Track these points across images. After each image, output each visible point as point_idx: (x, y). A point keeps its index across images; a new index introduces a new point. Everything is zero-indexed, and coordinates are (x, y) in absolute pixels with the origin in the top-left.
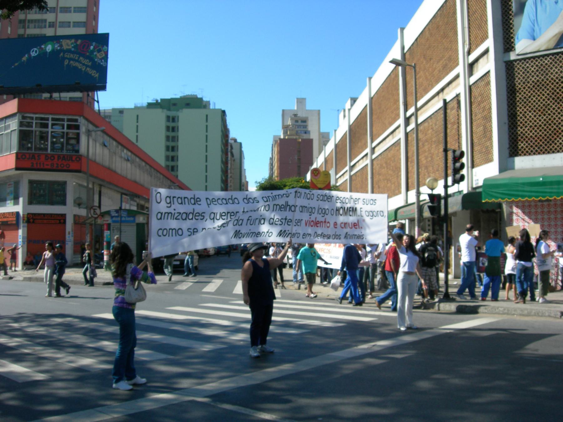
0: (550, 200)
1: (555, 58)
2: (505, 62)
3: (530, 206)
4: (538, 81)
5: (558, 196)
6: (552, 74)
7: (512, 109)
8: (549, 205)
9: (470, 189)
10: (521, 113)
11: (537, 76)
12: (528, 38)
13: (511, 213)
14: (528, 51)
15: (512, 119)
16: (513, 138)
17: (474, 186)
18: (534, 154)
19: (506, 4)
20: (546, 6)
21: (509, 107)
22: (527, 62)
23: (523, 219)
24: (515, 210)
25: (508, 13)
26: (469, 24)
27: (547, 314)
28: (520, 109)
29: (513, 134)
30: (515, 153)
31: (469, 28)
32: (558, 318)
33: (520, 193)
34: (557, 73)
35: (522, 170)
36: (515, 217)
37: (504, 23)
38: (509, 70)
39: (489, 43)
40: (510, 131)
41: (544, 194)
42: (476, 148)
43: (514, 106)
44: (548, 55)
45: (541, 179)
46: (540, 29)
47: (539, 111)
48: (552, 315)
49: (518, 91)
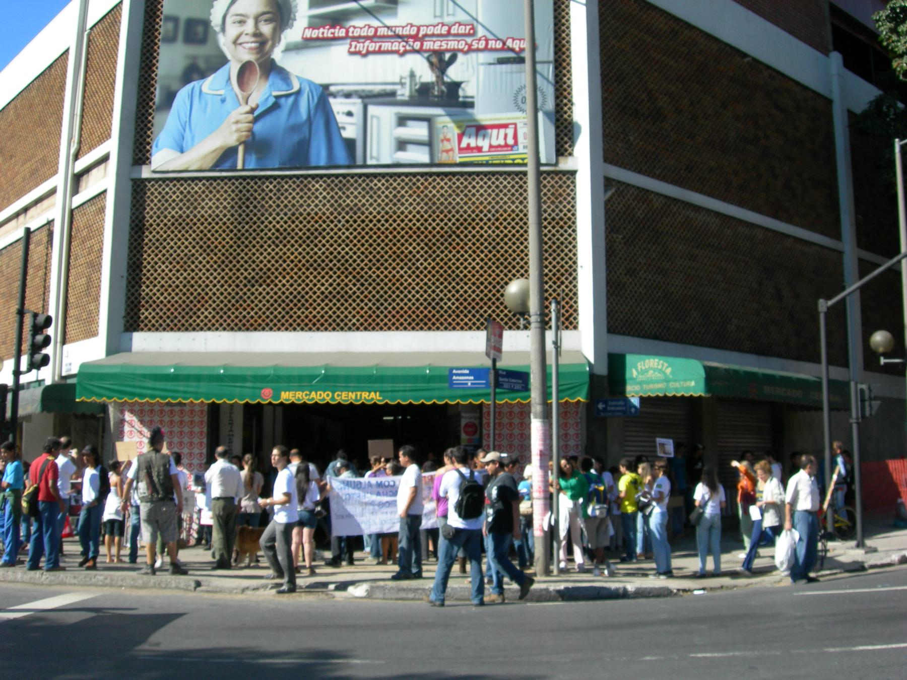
0: (185, 404)
2: (133, 180)
3: (152, 411)
4: (181, 216)
5: (197, 399)
6: (203, 208)
7: (135, 255)
8: (182, 411)
9: (56, 378)
10: (149, 263)
11: (181, 209)
12: (173, 148)
13: (122, 422)
14: (170, 169)
15: (134, 271)
16: (132, 302)
17: (64, 374)
18: (164, 329)
19: (146, 90)
20: (206, 105)
21: (131, 251)
22: (168, 185)
23: (140, 432)
24: (128, 416)
25: (148, 104)
26: (83, 110)
27: (174, 585)
28: (148, 258)
29: (133, 294)
30: (135, 326)
31: (82, 116)
32: (190, 590)
33: (137, 391)
34: (210, 208)
35: (142, 354)
36: (127, 428)
37: (139, 118)
38: (138, 193)
39: (111, 146)
40: (129, 291)
41: (174, 395)
42: (71, 312)
43: (139, 252)
44: (200, 179)
45: (172, 370)
46: (193, 138)
48: (182, 586)
49: (148, 229)
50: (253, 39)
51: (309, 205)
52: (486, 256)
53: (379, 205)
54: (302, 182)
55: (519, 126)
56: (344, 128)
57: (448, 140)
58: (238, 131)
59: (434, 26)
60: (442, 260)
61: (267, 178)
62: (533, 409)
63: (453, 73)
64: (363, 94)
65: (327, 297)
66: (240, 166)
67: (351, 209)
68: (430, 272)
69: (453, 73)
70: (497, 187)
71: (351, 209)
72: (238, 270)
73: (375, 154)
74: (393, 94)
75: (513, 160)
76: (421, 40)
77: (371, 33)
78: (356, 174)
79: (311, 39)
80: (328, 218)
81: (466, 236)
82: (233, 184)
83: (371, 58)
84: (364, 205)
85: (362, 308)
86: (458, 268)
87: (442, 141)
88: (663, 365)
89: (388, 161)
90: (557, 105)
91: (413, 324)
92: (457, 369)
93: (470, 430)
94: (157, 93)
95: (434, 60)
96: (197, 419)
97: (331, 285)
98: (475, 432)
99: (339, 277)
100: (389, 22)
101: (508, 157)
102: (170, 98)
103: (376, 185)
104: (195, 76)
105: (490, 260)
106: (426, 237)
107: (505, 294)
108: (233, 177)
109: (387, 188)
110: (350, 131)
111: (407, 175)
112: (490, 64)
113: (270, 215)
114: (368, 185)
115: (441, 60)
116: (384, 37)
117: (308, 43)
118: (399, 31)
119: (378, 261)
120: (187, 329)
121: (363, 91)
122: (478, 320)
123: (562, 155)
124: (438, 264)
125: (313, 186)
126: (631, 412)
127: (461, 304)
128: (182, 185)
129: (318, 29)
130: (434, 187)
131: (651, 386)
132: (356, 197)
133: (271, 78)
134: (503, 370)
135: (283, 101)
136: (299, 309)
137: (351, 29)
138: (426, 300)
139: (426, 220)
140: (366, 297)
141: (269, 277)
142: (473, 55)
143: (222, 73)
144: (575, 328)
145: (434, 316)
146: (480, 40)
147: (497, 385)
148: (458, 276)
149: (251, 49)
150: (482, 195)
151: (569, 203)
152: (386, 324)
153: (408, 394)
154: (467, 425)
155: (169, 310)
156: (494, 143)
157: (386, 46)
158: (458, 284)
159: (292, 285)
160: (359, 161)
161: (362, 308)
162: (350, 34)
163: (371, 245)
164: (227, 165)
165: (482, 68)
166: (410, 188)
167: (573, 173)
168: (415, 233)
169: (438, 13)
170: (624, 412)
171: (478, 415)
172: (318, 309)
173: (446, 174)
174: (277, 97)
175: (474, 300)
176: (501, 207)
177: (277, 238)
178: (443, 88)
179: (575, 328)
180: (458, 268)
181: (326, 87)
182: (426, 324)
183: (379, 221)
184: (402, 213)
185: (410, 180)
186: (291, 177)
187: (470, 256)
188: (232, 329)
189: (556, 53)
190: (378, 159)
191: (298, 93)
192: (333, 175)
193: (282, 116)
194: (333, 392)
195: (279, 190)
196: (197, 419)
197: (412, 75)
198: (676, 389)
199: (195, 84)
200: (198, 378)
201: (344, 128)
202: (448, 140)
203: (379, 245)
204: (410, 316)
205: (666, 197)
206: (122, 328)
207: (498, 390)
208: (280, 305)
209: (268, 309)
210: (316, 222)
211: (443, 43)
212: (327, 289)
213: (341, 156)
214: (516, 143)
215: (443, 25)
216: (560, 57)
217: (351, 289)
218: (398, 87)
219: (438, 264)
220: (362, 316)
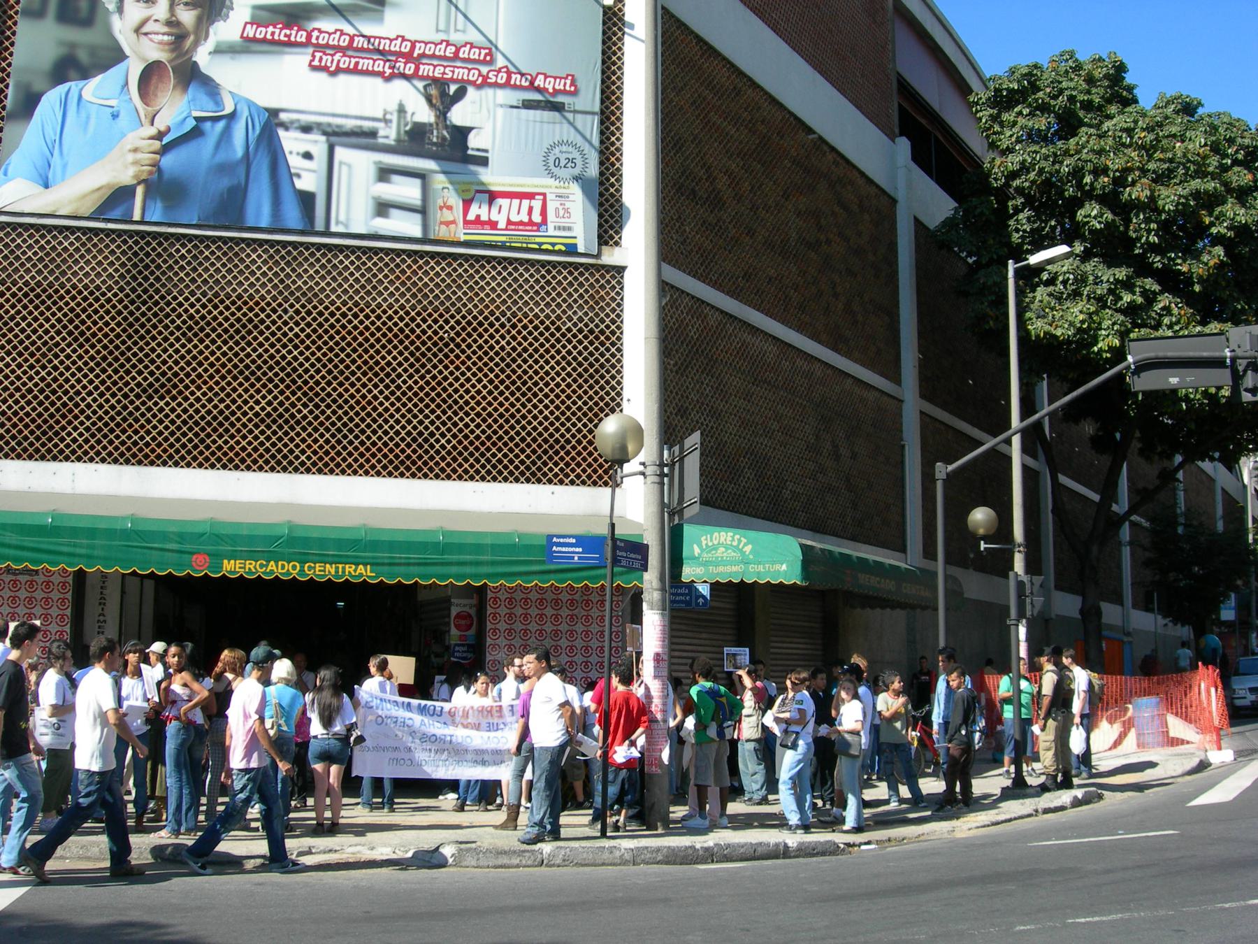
1: (90, 239)
4: (39, 284)
6: (75, 274)
20: (88, 118)
22: (19, 235)
34: (87, 275)
46: (65, 166)
50: (166, 29)
51: (240, 284)
52: (497, 376)
53: (345, 292)
54: (231, 248)
56: (299, 176)
57: (450, 208)
58: (135, 163)
59: (436, 45)
60: (434, 378)
62: (645, 596)
63: (459, 115)
64: (329, 130)
65: (263, 421)
66: (137, 217)
67: (304, 294)
68: (416, 394)
69: (459, 115)
70: (515, 280)
71: (304, 294)
72: (128, 372)
73: (342, 218)
74: (373, 134)
75: (540, 244)
76: (417, 61)
77: (344, 42)
78: (313, 244)
79: (254, 40)
80: (269, 304)
81: (469, 346)
82: (125, 242)
83: (342, 78)
84: (322, 290)
85: (316, 441)
86: (456, 391)
87: (441, 208)
88: (739, 540)
89: (363, 231)
90: (602, 174)
92: (558, 537)
93: (463, 622)
94: (10, 92)
95: (433, 91)
97: (269, 403)
98: (469, 627)
99: (282, 392)
100: (368, 29)
101: (532, 240)
102: (30, 102)
103: (341, 262)
104: (72, 73)
105: (502, 382)
106: (412, 343)
107: (596, 432)
108: (125, 232)
109: (358, 269)
110: (308, 181)
111: (387, 252)
112: (512, 107)
113: (181, 293)
114: (329, 261)
115: (443, 94)
116: (362, 50)
117: (249, 46)
118: (385, 45)
119: (342, 373)
120: (43, 458)
121: (329, 125)
122: (483, 466)
123: (606, 243)
124: (428, 383)
125: (248, 256)
126: (698, 604)
127: (460, 442)
128: (43, 236)
129: (267, 27)
130: (426, 273)
131: (721, 569)
132: (311, 277)
133: (191, 90)
134: (621, 540)
135: (207, 126)
137: (315, 34)
138: (409, 434)
139: (413, 319)
140: (321, 424)
141: (175, 386)
142: (489, 92)
143: (115, 73)
145: (420, 457)
146: (499, 71)
147: (616, 561)
148: (456, 402)
149: (161, 43)
150: (493, 290)
151: (613, 310)
152: (350, 466)
154: (458, 616)
155: (15, 426)
156: (514, 218)
157: (365, 64)
158: (456, 413)
159: (210, 400)
160: (320, 226)
161: (316, 441)
162: (314, 41)
163: (331, 349)
164: (116, 214)
165: (500, 111)
166: (392, 271)
167: (621, 270)
168: (396, 336)
169: (442, 27)
170: (688, 603)
171: (474, 601)
172: (250, 438)
173: (444, 256)
174: (196, 119)
175: (478, 438)
176: (520, 309)
177: (190, 328)
178: (445, 133)
180: (456, 391)
181: (274, 113)
182: (408, 469)
183: (344, 315)
184: (379, 306)
185: (392, 260)
186: (214, 240)
187: (474, 375)
188: (116, 461)
189: (602, 102)
190: (346, 226)
191: (232, 116)
192: (278, 242)
193: (204, 150)
194: (303, 563)
195: (195, 258)
196: (55, 595)
197: (401, 110)
199: (74, 86)
200: (91, 533)
201: (299, 176)
202: (450, 208)
203: (343, 350)
204: (385, 456)
205: (722, 312)
207: (616, 569)
208: (191, 429)
209: (172, 433)
210: (251, 309)
211: (447, 70)
212: (263, 409)
213: (292, 216)
214: (544, 221)
215: (448, 44)
216: (607, 108)
217: (299, 411)
218: (380, 125)
219: (428, 383)
220: (315, 453)
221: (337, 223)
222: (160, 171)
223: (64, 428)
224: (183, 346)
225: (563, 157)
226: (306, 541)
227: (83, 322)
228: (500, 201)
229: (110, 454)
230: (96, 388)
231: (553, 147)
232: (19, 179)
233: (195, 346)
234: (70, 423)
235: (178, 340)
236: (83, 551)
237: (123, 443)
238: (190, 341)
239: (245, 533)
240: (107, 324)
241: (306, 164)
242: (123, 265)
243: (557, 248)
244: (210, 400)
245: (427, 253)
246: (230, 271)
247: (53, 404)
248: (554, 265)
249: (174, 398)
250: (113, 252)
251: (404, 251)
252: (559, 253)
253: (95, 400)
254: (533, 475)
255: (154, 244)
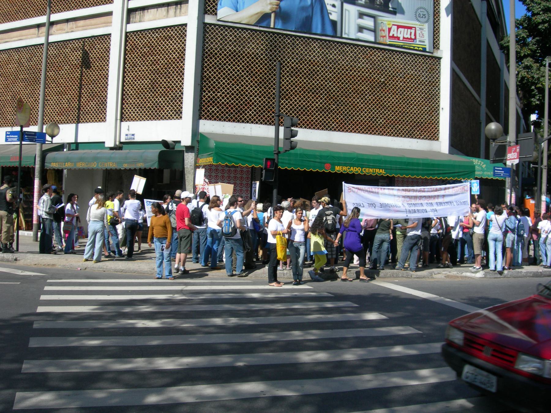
3: (217, 170)
4: (235, 51)
8: (236, 171)
9: (117, 143)
14: (230, 21)
17: (123, 140)
22: (227, 30)
33: (254, 160)
34: (253, 48)
44: (247, 30)
47: (233, 80)
48: (405, 276)
55: (417, 29)
61: (287, 35)
66: (272, 26)
72: (270, 89)
73: (347, 32)
75: (414, 47)
82: (267, 36)
87: (381, 30)
88: (481, 163)
89: (354, 38)
91: (323, 126)
96: (244, 176)
103: (346, 49)
108: (267, 32)
111: (362, 46)
113: (289, 58)
136: (304, 115)
144: (437, 139)
153: (398, 171)
156: (406, 36)
160: (339, 35)
164: (264, 24)
167: (440, 58)
173: (381, 49)
179: (437, 139)
186: (300, 37)
188: (266, 124)
194: (362, 168)
196: (244, 176)
198: (488, 175)
201: (331, 14)
202: (384, 31)
206: (198, 117)
214: (415, 38)
221: (345, 34)
222: (280, 8)
223: (246, 110)
224: (290, 79)
225: (421, 13)
226: (362, 160)
227: (252, 67)
228: (400, 29)
229: (264, 121)
230: (258, 94)
231: (418, 9)
232: (226, 7)
233: (294, 79)
234: (248, 108)
235: (288, 76)
236: (287, 162)
237: (268, 117)
238: (292, 77)
239: (342, 156)
240: (261, 69)
241: (333, 9)
242: (267, 45)
243: (420, 49)
244: (300, 101)
245: (375, 48)
246: (306, 50)
247: (242, 100)
248: (418, 55)
249: (287, 100)
250: (262, 40)
251: (367, 46)
252: (420, 51)
253: (258, 99)
254: (410, 135)
255: (278, 37)
